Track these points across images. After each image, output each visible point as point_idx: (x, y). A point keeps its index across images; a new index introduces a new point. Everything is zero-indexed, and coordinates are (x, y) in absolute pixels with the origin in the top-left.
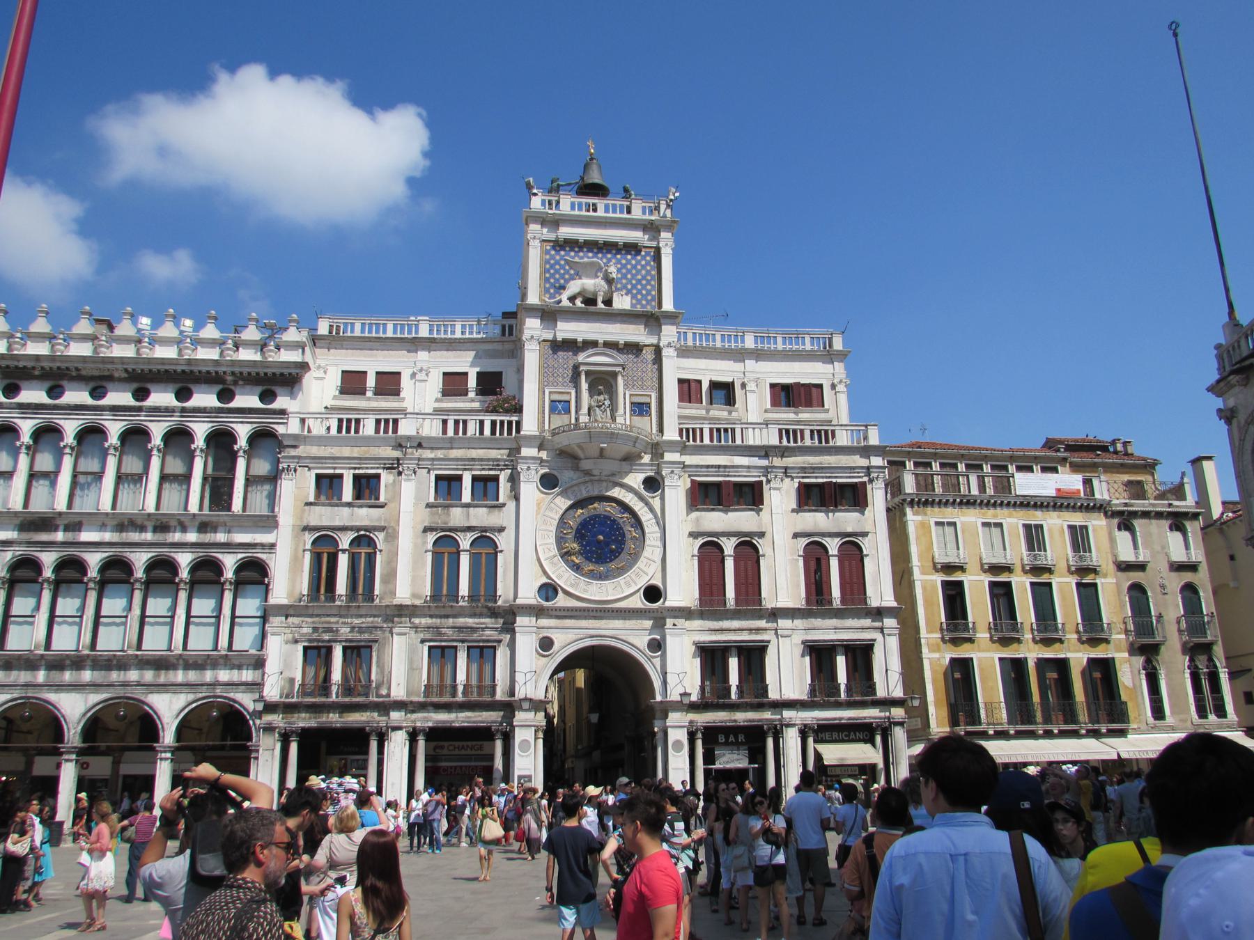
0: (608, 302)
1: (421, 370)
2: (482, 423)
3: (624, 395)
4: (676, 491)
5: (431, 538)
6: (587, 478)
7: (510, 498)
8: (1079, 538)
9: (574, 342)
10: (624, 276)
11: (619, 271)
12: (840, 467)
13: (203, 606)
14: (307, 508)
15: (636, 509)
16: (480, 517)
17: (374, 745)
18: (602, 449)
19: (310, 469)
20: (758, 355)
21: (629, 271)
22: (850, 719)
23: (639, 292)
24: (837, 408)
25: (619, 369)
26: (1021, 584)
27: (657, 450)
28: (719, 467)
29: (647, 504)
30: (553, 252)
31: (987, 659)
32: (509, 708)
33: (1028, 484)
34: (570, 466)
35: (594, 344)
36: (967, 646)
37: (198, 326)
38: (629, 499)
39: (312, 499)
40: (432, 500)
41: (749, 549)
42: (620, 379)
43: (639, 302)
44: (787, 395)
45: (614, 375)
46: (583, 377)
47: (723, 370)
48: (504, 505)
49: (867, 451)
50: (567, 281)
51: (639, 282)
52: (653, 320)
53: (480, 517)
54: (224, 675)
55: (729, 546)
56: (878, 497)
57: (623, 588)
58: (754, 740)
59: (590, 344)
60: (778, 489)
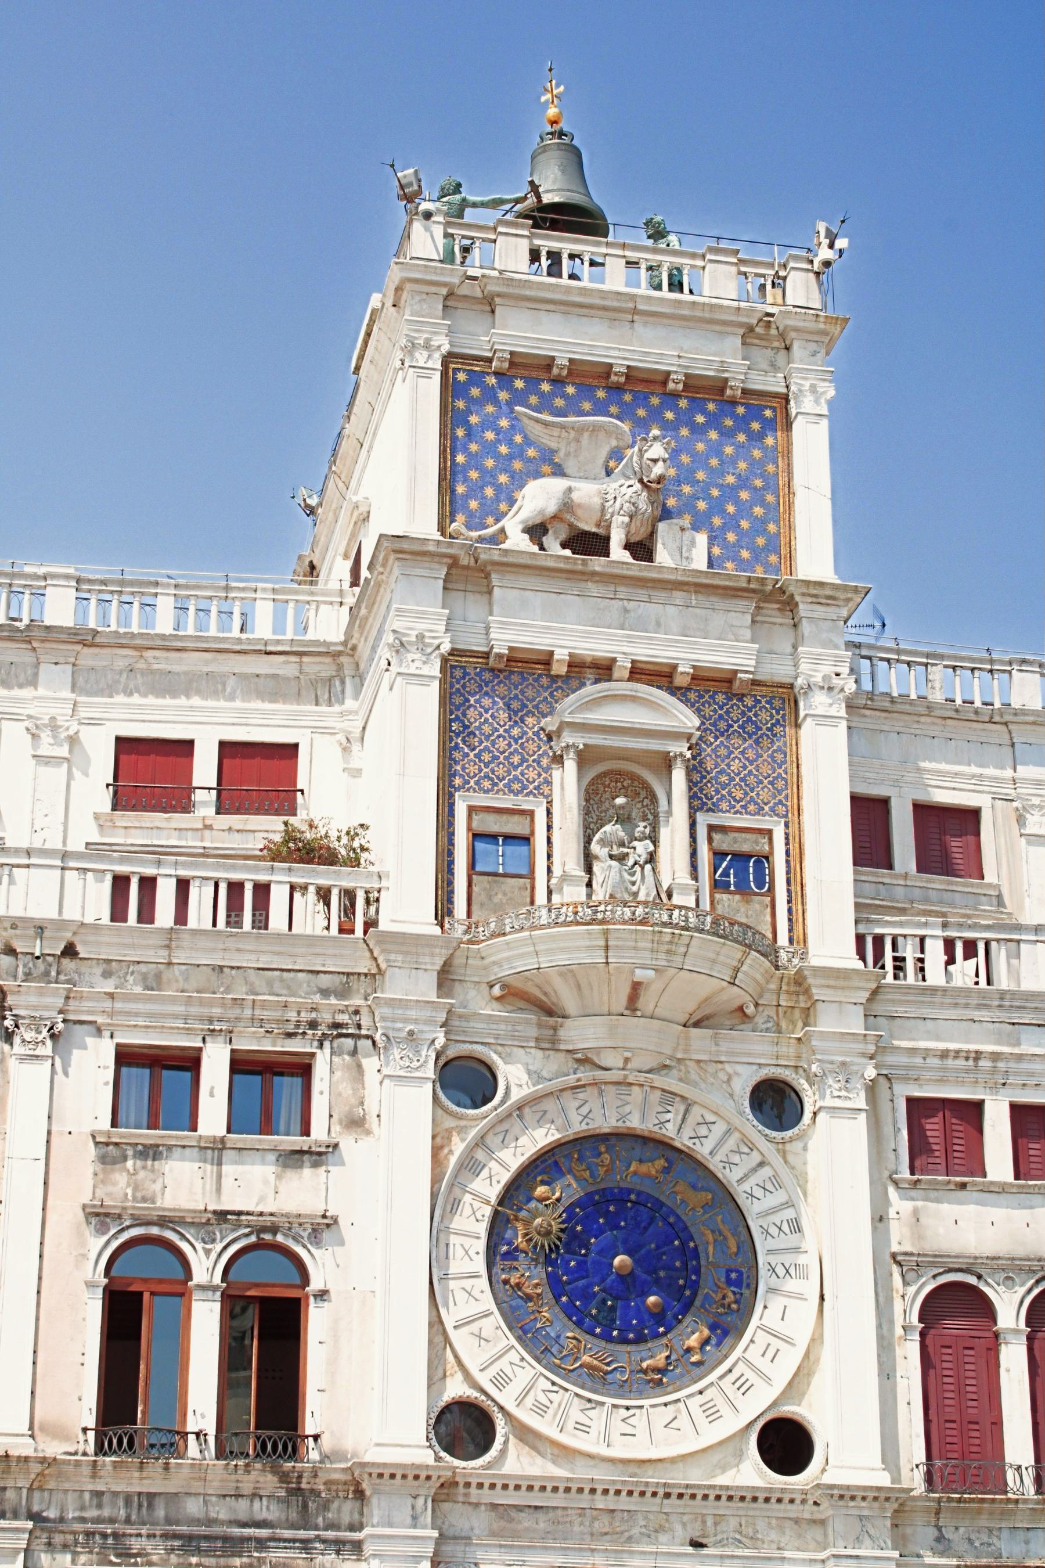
0: (642, 549)
2: (262, 891)
6: (585, 1075)
9: (546, 660)
10: (687, 476)
15: (731, 1177)
18: (636, 987)
21: (701, 461)
23: (732, 523)
25: (681, 748)
28: (978, 1055)
35: (604, 669)
43: (732, 553)
46: (570, 764)
50: (519, 481)
51: (730, 493)
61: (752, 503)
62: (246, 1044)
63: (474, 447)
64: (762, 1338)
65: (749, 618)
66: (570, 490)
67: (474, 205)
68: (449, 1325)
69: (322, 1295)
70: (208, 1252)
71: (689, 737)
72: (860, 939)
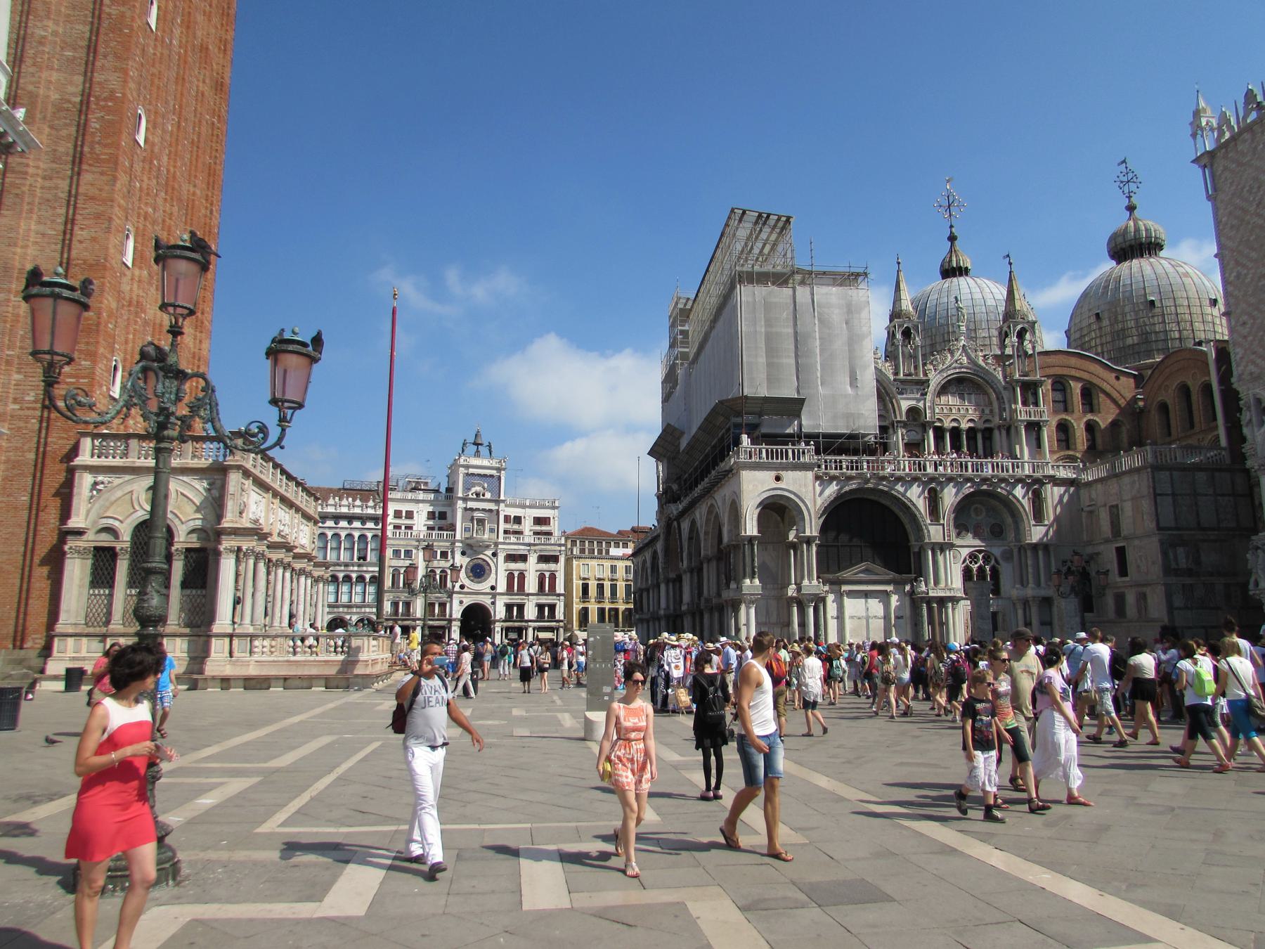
3: (487, 526)
4: (501, 557)
12: (550, 550)
13: (359, 589)
20: (530, 507)
24: (554, 527)
26: (607, 584)
31: (593, 607)
32: (450, 621)
33: (614, 551)
34: (470, 548)
37: (354, 500)
41: (522, 576)
44: (539, 521)
49: (560, 545)
52: (498, 502)
54: (368, 610)
55: (516, 574)
56: (562, 559)
57: (485, 586)
58: (520, 631)
59: (478, 509)
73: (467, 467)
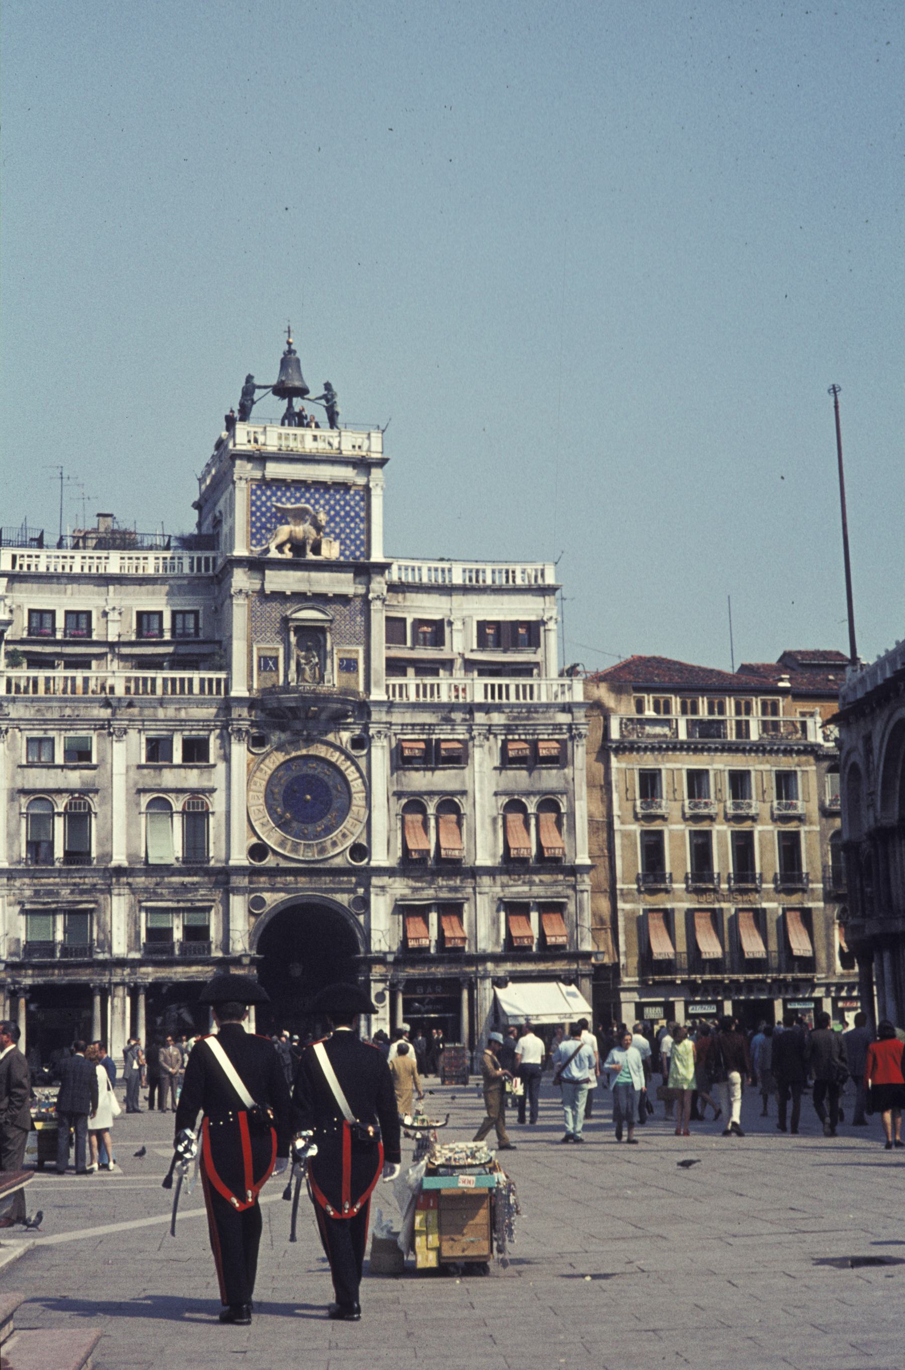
0: (317, 550)
1: (114, 609)
5: (145, 799)
7: (219, 757)
8: (785, 782)
9: (284, 593)
10: (332, 519)
11: (328, 513)
14: (19, 770)
16: (192, 778)
17: (98, 999)
19: (20, 730)
20: (465, 590)
22: (540, 971)
27: (364, 709)
28: (424, 725)
29: (354, 763)
30: (259, 492)
36: (662, 896)
38: (335, 757)
39: (24, 762)
40: (143, 761)
42: (328, 635)
43: (347, 547)
45: (323, 630)
47: (430, 607)
48: (214, 766)
53: (192, 778)
60: (481, 746)
61: (355, 528)
62: (186, 733)
63: (258, 514)
64: (351, 820)
65: (351, 575)
66: (291, 532)
67: (260, 387)
68: (252, 820)
69: (213, 813)
70: (177, 801)
71: (331, 621)
72: (387, 686)
73: (260, 459)
